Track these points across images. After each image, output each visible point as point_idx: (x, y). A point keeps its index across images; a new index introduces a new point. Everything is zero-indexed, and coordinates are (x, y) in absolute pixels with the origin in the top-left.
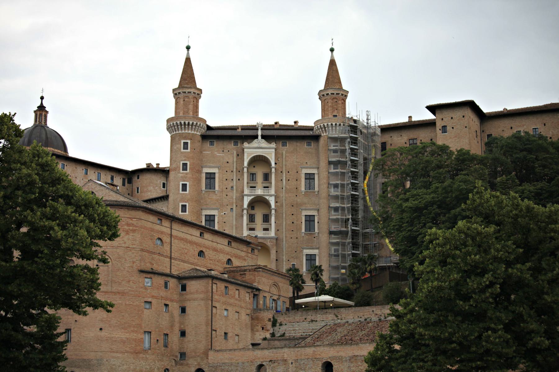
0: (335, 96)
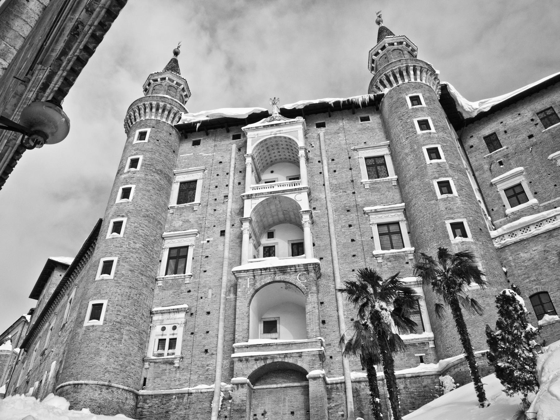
0: (396, 46)
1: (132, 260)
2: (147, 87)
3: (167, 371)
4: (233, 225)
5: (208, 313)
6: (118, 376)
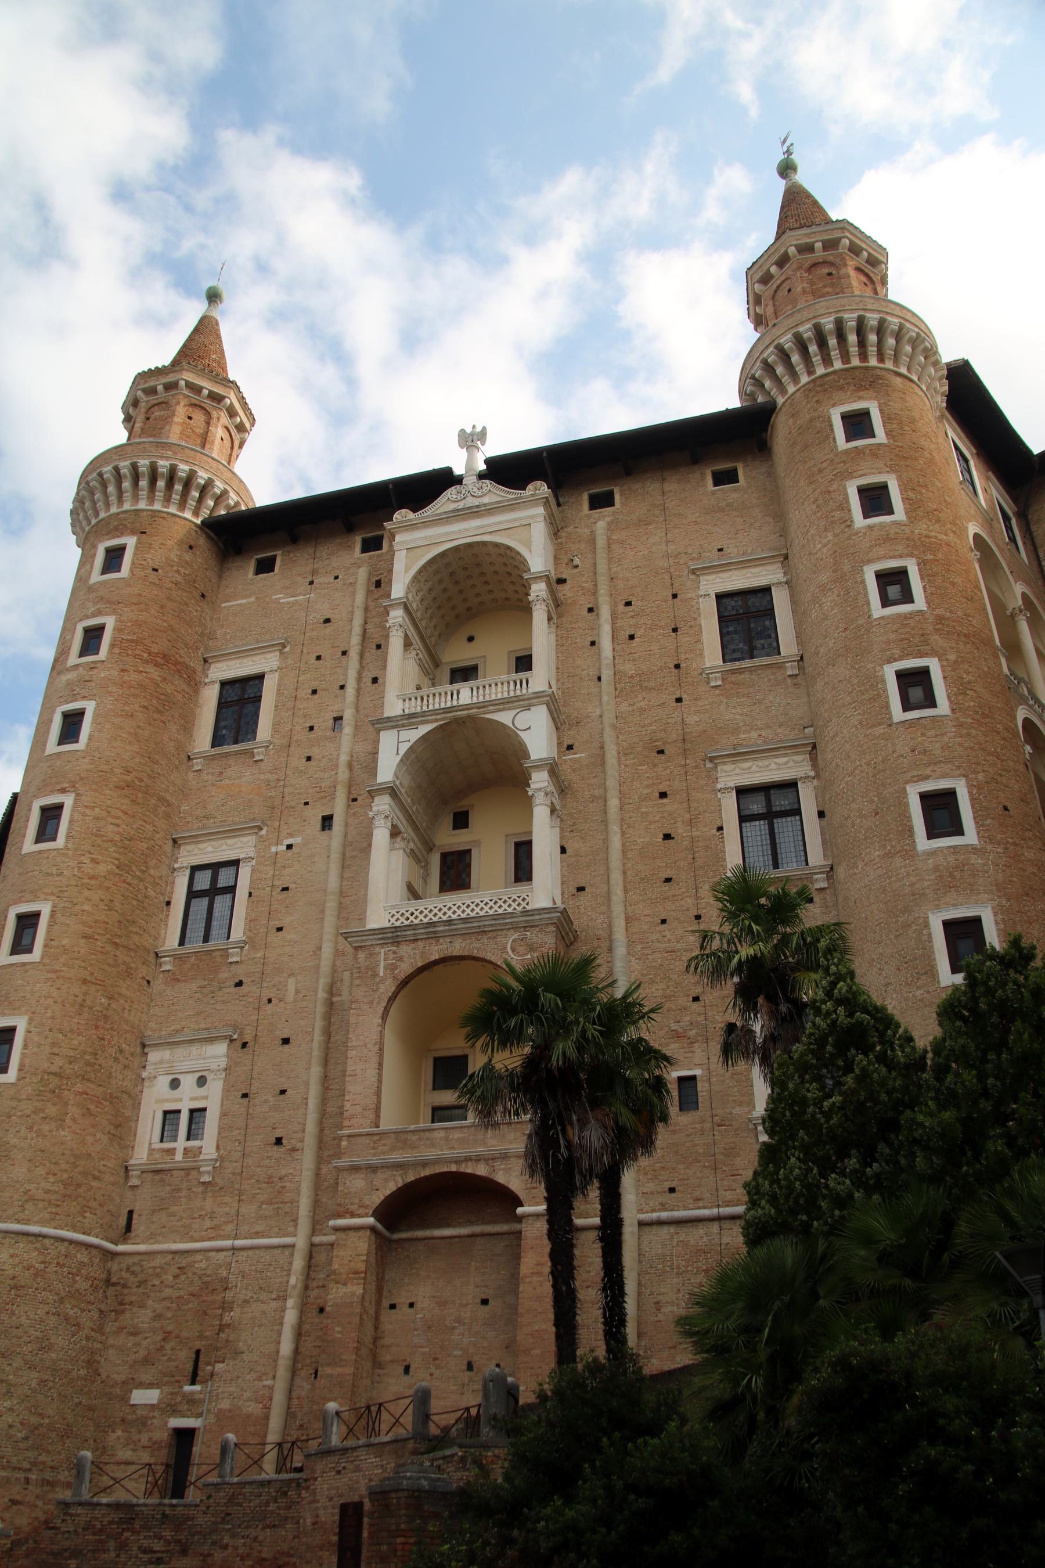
0: (819, 253)
1: (87, 907)
2: (131, 410)
3: (184, 1193)
4: (355, 800)
5: (286, 1041)
6: (58, 1210)
